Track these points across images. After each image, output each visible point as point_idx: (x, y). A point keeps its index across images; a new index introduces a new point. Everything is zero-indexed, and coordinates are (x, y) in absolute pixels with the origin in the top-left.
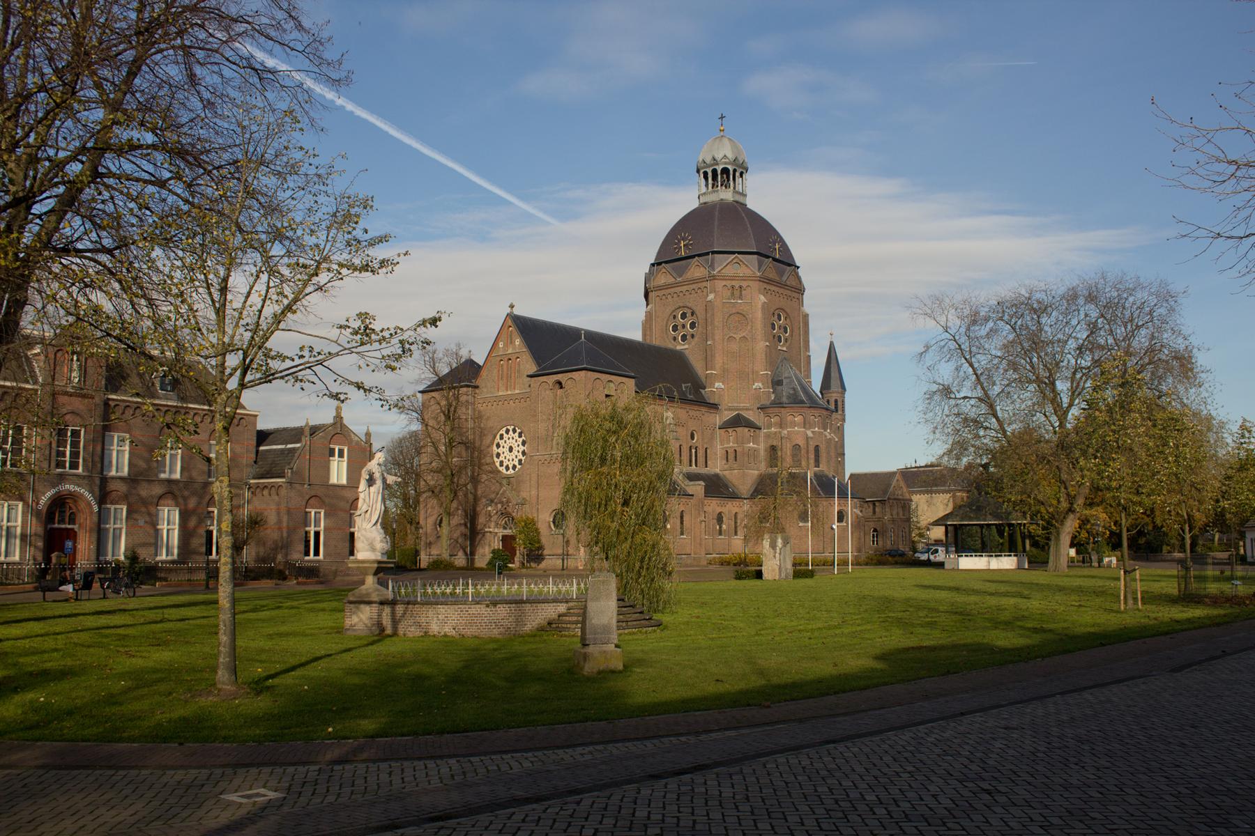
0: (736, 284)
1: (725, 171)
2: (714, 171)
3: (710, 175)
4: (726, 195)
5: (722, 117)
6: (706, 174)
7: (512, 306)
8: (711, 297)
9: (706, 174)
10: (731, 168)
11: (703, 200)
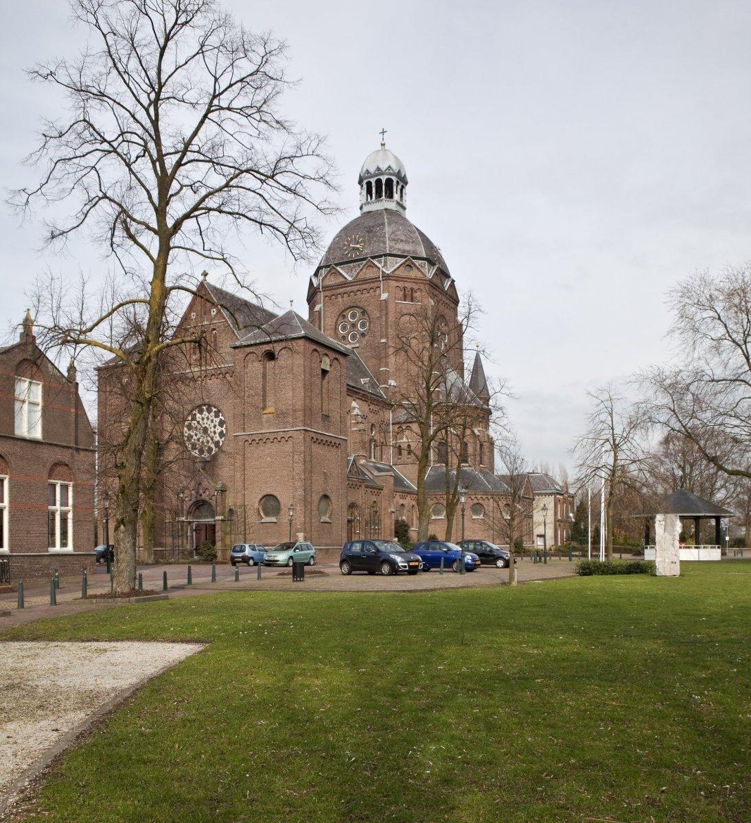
0: (409, 285)
1: (389, 182)
2: (379, 182)
3: (374, 184)
4: (392, 205)
5: (383, 132)
6: (369, 184)
7: (205, 274)
8: (384, 296)
9: (369, 184)
10: (394, 179)
11: (366, 209)
